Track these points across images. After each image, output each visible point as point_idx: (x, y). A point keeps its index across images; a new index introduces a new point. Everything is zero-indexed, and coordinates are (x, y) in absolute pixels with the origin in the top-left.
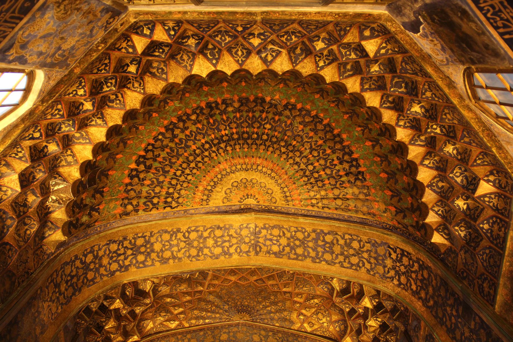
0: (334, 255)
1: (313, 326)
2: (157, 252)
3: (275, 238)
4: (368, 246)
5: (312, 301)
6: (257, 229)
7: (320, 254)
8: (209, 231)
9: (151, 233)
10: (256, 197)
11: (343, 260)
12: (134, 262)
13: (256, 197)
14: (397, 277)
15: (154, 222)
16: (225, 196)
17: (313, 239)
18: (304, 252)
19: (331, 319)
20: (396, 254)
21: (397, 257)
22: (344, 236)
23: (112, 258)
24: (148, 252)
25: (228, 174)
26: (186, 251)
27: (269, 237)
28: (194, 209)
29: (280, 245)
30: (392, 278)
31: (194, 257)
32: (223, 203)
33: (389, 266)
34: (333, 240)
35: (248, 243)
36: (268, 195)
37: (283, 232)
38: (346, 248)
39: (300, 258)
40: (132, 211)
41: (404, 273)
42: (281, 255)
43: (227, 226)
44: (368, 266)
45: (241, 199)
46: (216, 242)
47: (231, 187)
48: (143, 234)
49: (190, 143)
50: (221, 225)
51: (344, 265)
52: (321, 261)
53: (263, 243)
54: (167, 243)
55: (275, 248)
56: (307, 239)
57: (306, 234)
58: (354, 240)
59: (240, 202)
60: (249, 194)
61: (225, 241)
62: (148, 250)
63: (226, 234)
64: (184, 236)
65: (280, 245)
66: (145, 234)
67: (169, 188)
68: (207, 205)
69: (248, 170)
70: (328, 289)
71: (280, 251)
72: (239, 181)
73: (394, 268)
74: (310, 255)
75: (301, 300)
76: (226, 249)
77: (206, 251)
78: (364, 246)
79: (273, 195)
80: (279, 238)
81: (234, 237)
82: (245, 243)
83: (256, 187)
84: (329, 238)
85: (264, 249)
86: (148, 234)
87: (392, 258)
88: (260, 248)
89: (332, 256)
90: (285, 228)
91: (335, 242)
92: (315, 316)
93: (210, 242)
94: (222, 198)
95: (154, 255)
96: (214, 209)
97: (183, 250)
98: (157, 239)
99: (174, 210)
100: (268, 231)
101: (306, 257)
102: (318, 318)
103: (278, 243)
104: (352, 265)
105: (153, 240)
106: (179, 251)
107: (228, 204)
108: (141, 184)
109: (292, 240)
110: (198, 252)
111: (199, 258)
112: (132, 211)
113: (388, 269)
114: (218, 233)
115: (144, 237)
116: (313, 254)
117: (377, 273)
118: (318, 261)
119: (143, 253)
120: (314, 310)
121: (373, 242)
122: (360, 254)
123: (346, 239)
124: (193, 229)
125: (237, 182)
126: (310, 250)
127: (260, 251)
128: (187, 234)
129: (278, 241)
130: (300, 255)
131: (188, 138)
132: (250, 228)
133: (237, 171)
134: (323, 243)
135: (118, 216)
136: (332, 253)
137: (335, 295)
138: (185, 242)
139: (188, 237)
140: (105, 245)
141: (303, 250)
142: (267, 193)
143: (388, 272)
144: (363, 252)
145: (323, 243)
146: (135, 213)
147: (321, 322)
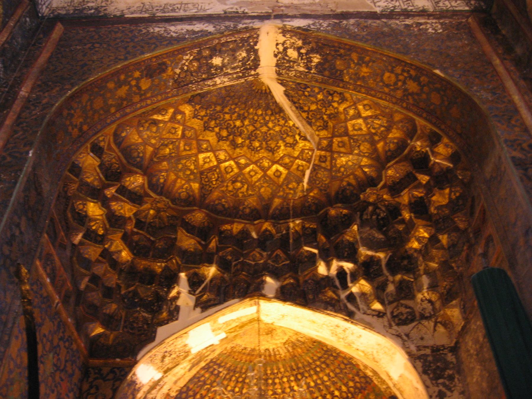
49: (312, 384)
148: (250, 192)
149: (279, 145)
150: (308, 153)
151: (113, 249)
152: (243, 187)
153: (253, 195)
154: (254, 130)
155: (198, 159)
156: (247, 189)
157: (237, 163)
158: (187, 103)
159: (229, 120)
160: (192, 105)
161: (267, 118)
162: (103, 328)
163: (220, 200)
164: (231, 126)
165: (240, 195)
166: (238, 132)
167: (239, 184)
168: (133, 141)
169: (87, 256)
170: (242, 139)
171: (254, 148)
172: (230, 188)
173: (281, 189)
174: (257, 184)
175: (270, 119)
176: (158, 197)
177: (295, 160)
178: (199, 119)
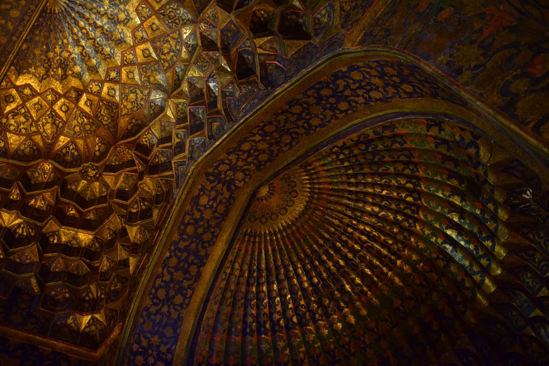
0: (172, 270)
1: (6, 101)
2: (312, 105)
3: (215, 205)
4: (175, 315)
5: (49, 120)
6: (233, 187)
7: (179, 254)
8: (276, 152)
9: (337, 118)
10: (264, 200)
11: (164, 279)
12: (331, 86)
13: (264, 200)
14: (140, 350)
15: (344, 128)
16: (292, 179)
17: (198, 251)
18: (187, 235)
19: (10, 132)
20: (165, 351)
21: (163, 354)
22: (191, 289)
23: (368, 84)
24: (323, 100)
25: (311, 197)
26: (279, 124)
27: (220, 197)
28: (310, 156)
29: (206, 208)
30: (139, 342)
31: (265, 125)
32: (286, 174)
33: (152, 339)
34: (190, 275)
35: (226, 172)
36: (261, 215)
37: (217, 218)
38: (177, 286)
39: (182, 227)
40: (383, 132)
41: (146, 360)
42: (194, 205)
43: (262, 167)
44: (153, 309)
45: (273, 187)
46: (256, 150)
47: (295, 189)
48: (347, 114)
50: (268, 164)
51: (158, 279)
52: (170, 252)
53: (215, 187)
54: (307, 117)
55: (204, 200)
56: (200, 244)
57: (207, 245)
58: (184, 300)
59: (273, 184)
60: (272, 196)
61: (248, 157)
62: (324, 102)
63: (255, 161)
64: (297, 133)
65: (206, 208)
66: (344, 114)
67: (357, 160)
68: (301, 165)
69: (299, 216)
70: (65, 155)
71: (199, 205)
72: (294, 199)
73: (150, 346)
74: (181, 241)
75: (56, 108)
76: (240, 153)
77: (258, 138)
78: (176, 310)
79: (258, 221)
80: (213, 210)
81: (244, 166)
82: (230, 170)
83: (276, 208)
84: (193, 270)
85: (209, 186)
86: (340, 116)
87: (160, 346)
88: (211, 182)
89: (172, 268)
90: (221, 222)
91: (188, 276)
92: (23, 111)
93: (262, 146)
94: (292, 177)
95: (312, 101)
96: (291, 166)
97: (282, 123)
98: (325, 116)
99: (333, 145)
100: (226, 199)
101: (181, 235)
102: (17, 114)
103: (208, 206)
104: (157, 290)
105: (329, 113)
106: (286, 121)
107: (281, 176)
108: (394, 158)
109: (206, 225)
110: (264, 131)
111: (258, 129)
112: (383, 132)
113: (148, 338)
114: (263, 157)
115: (342, 112)
116: (182, 245)
117: (144, 321)
118: (173, 248)
119: (328, 97)
120: (34, 115)
121: (179, 323)
122: (167, 302)
123: (187, 291)
124: (294, 143)
125: (294, 197)
126: (186, 243)
127: (208, 180)
128: (294, 136)
129: (211, 207)
130: (185, 228)
131: (383, 213)
132: (240, 181)
133: (305, 206)
134: (190, 261)
135: (397, 125)
136: (176, 268)
137: (56, 165)
138: (289, 129)
139: (290, 134)
140: (392, 97)
141: (190, 234)
142: (263, 216)
143: (146, 338)
144: (169, 307)
145: (190, 261)
146: (375, 130)
147: (10, 116)
148: (146, 92)
149: (120, 31)
150: (143, 8)
151: (64, 239)
152: (137, 94)
153: (150, 91)
154: (94, 42)
155: (82, 109)
156: (142, 92)
157: (111, 81)
158: (19, 75)
159: (69, 56)
160: (25, 73)
161: (91, 22)
162: (87, 315)
163: (132, 122)
164: (76, 58)
165: (142, 103)
166: (84, 57)
167: (132, 96)
168: (18, 142)
169: (28, 261)
170: (94, 58)
171: (109, 55)
172: (129, 106)
173: (162, 62)
174: (143, 79)
175: (93, 19)
176: (80, 168)
177: (143, 25)
178: (45, 79)
